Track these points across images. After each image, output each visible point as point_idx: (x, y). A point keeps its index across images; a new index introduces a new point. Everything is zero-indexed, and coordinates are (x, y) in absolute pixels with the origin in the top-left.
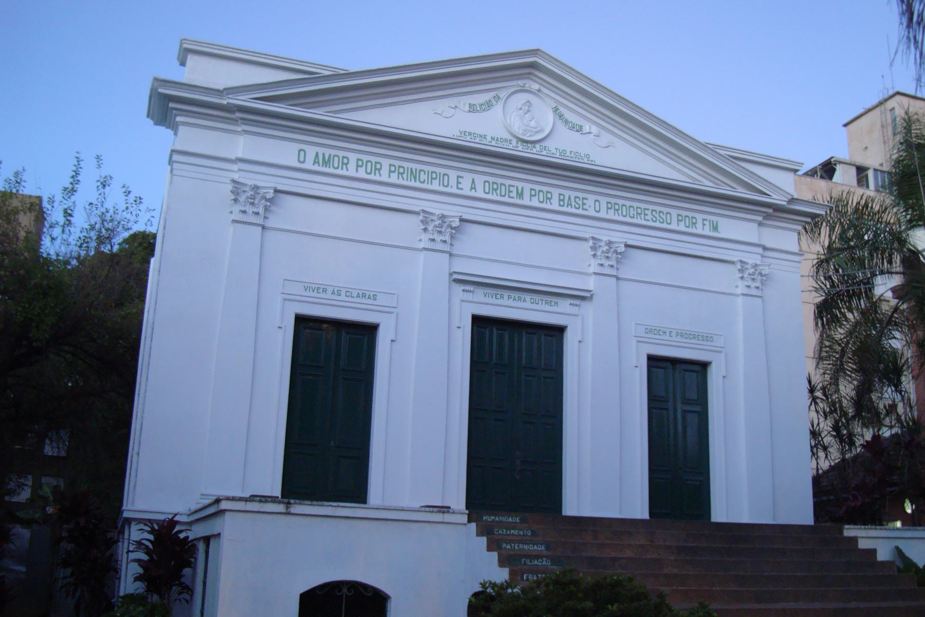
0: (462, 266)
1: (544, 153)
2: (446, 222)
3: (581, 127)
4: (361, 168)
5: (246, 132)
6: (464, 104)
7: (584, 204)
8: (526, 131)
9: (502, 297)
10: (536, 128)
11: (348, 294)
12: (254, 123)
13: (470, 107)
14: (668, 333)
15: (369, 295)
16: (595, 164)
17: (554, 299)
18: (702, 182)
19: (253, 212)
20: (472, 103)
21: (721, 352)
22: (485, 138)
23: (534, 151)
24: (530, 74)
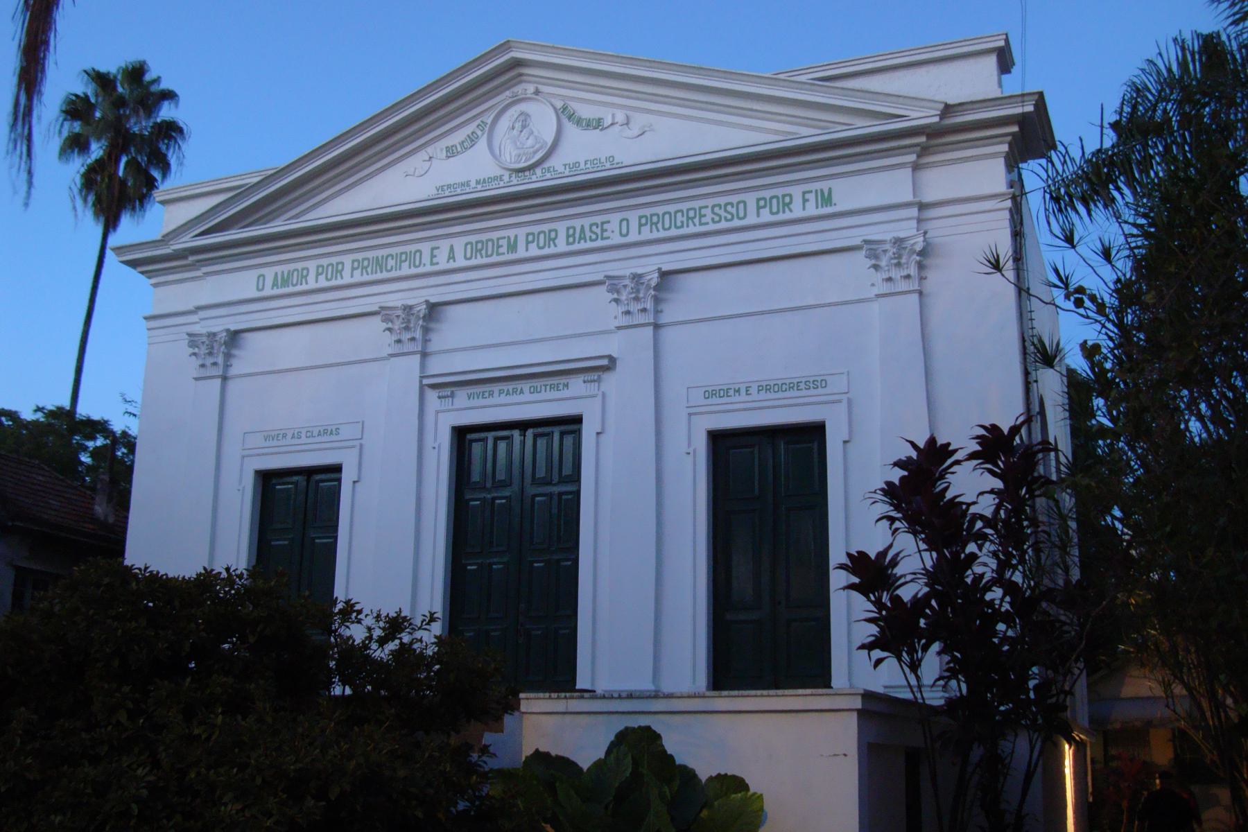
0: (437, 366)
1: (548, 176)
2: (907, 247)
3: (599, 121)
4: (764, 209)
5: (207, 274)
6: (442, 150)
7: (603, 231)
8: (519, 156)
9: (491, 394)
10: (533, 147)
11: (309, 434)
12: (310, 245)
13: (447, 151)
14: (743, 391)
15: (332, 430)
16: (623, 165)
17: (562, 380)
18: (906, 116)
19: (901, 277)
20: (450, 144)
21: (840, 401)
22: (468, 185)
23: (534, 178)
24: (521, 75)
